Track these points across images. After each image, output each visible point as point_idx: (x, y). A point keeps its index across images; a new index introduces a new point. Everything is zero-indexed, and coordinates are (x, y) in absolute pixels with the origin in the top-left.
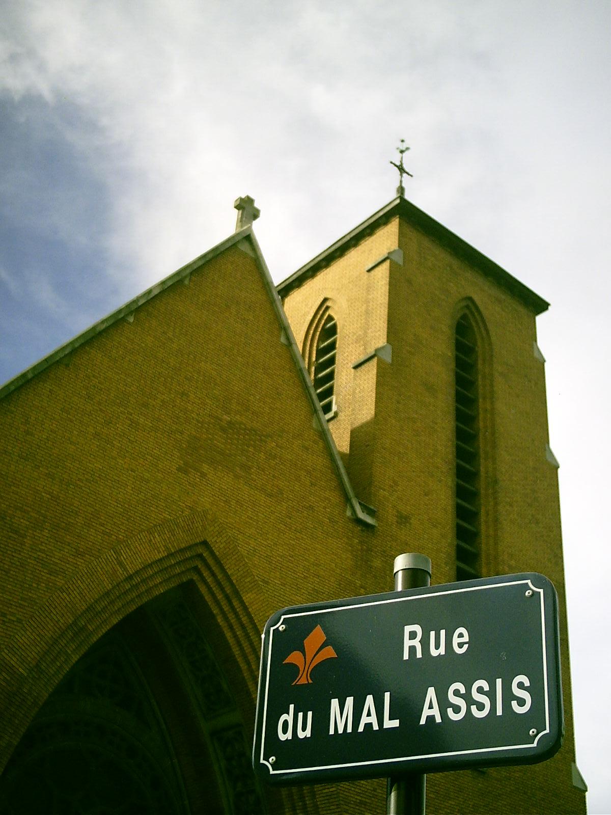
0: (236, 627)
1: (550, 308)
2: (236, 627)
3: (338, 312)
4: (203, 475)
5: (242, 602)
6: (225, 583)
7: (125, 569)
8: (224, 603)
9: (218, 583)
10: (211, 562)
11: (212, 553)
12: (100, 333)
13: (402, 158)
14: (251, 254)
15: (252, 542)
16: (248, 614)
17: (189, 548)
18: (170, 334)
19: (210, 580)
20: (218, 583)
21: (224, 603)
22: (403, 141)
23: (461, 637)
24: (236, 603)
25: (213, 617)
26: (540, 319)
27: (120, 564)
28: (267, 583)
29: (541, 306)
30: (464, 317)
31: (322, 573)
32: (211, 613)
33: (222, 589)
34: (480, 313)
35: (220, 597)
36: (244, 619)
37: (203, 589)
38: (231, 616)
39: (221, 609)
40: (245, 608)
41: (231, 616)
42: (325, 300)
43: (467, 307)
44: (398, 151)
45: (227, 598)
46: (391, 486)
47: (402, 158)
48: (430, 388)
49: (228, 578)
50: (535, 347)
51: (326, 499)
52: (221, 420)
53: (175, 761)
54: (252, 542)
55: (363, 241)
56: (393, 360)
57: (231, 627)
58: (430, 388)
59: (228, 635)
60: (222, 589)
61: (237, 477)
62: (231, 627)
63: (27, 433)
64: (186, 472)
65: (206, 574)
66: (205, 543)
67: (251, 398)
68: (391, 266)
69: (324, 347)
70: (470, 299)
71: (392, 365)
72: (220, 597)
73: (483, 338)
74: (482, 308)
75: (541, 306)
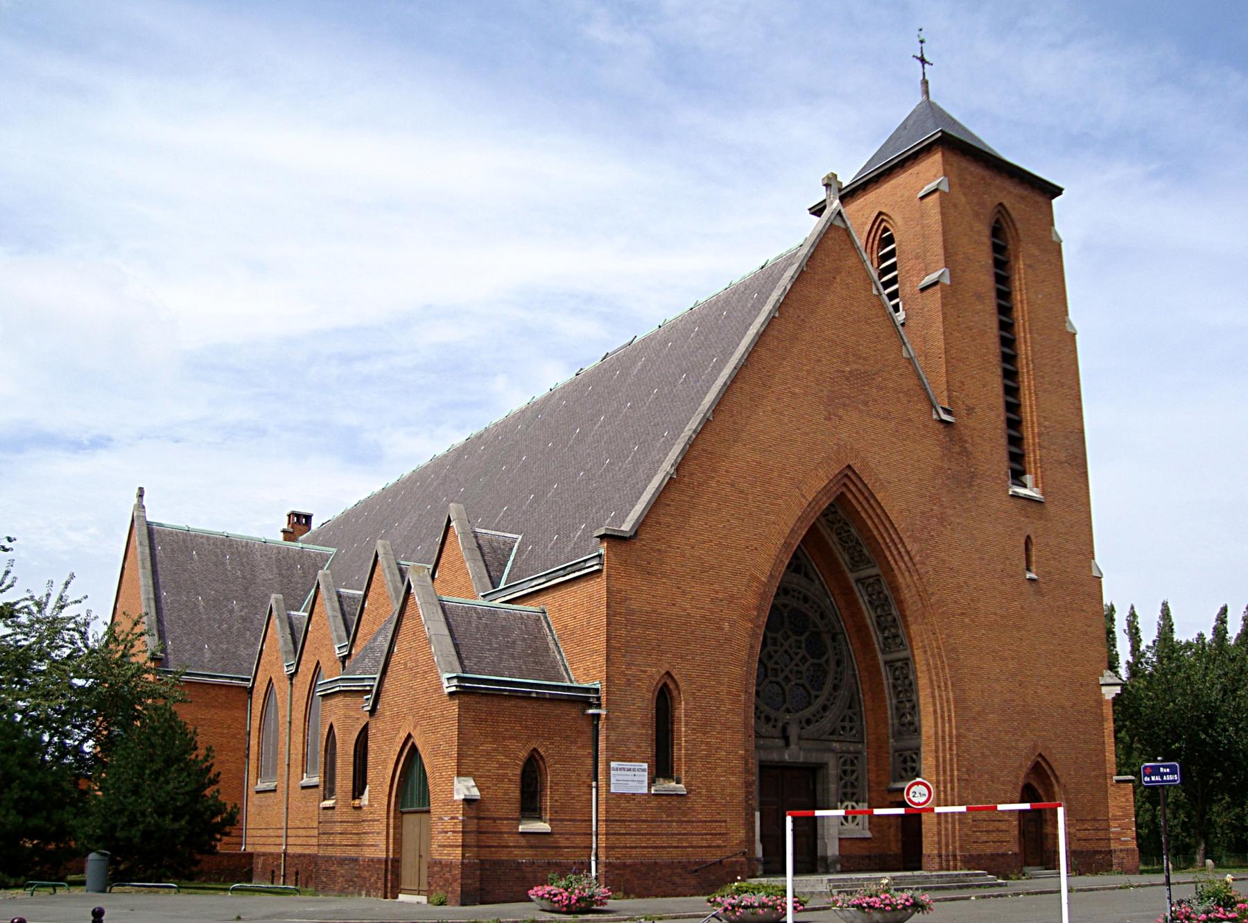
0: (874, 516)
1: (1064, 192)
2: (874, 516)
3: (899, 229)
4: (840, 418)
5: (876, 500)
6: (864, 490)
7: (807, 500)
8: (864, 503)
9: (860, 491)
10: (853, 477)
11: (854, 472)
12: (762, 335)
13: (922, 48)
14: (842, 225)
15: (877, 457)
16: (881, 507)
17: (840, 473)
18: (802, 317)
19: (854, 489)
20: (860, 491)
21: (864, 503)
22: (921, 30)
23: (1168, 770)
24: (872, 501)
25: (858, 513)
26: (1055, 202)
27: (803, 496)
28: (889, 483)
29: (1058, 191)
30: (997, 221)
31: (922, 466)
32: (857, 511)
33: (863, 494)
34: (1009, 215)
35: (861, 499)
36: (879, 511)
37: (850, 496)
38: (870, 511)
39: (863, 508)
40: (879, 504)
41: (870, 511)
42: (880, 213)
43: (999, 212)
44: (918, 40)
45: (866, 499)
46: (960, 387)
47: (922, 48)
48: (979, 297)
49: (865, 485)
50: (1053, 232)
51: (919, 410)
52: (843, 372)
53: (832, 599)
54: (877, 457)
55: (909, 164)
56: (951, 282)
57: (870, 517)
58: (979, 297)
59: (869, 522)
60: (863, 494)
61: (860, 411)
62: (870, 517)
63: (735, 423)
64: (830, 419)
65: (851, 486)
66: (849, 466)
67: (861, 347)
68: (940, 197)
69: (884, 254)
70: (1001, 204)
71: (950, 286)
72: (861, 499)
73: (1013, 238)
74: (1010, 210)
75: (1058, 191)
